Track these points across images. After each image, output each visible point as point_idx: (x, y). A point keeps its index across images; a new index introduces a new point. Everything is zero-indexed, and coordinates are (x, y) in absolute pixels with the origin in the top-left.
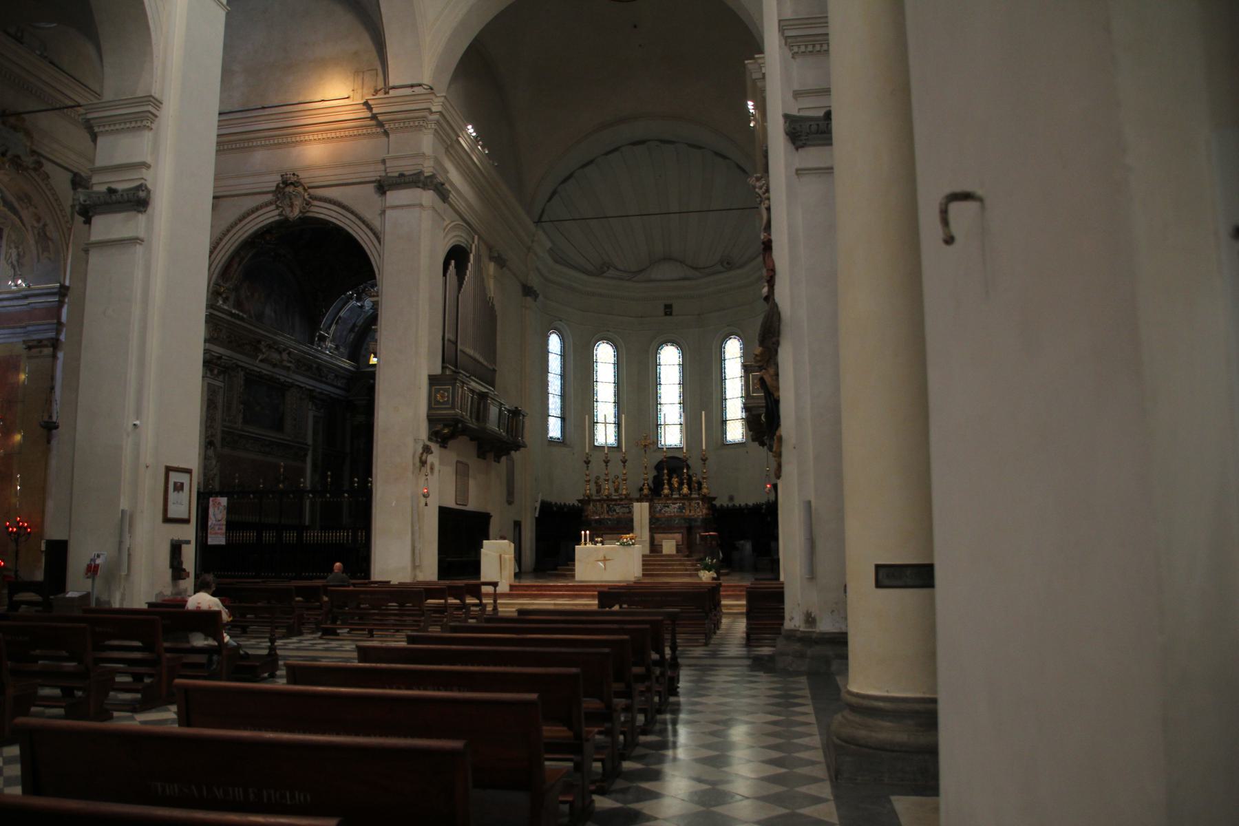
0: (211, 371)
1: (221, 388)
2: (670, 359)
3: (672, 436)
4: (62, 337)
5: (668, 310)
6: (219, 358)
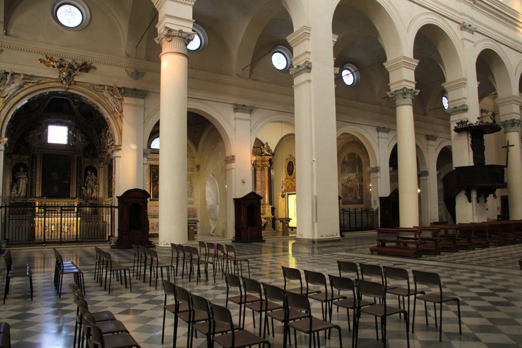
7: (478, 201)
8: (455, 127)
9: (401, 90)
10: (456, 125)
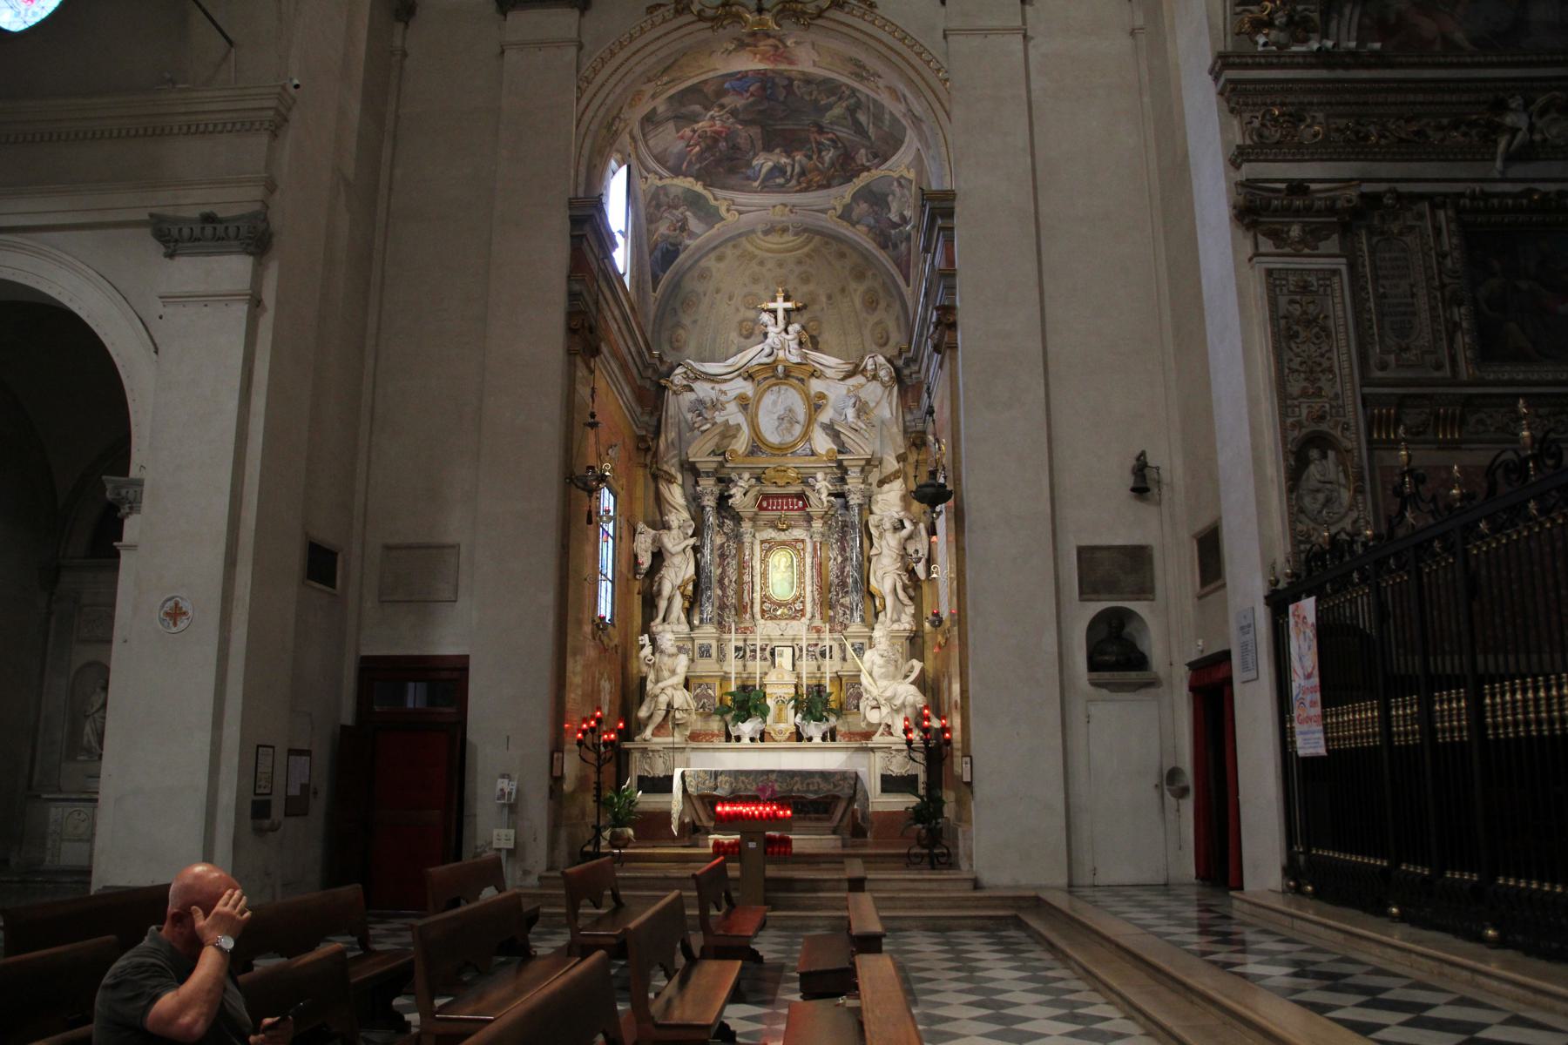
0: (1277, 236)
1: (1335, 272)
4: (958, 304)
6: (1298, 188)
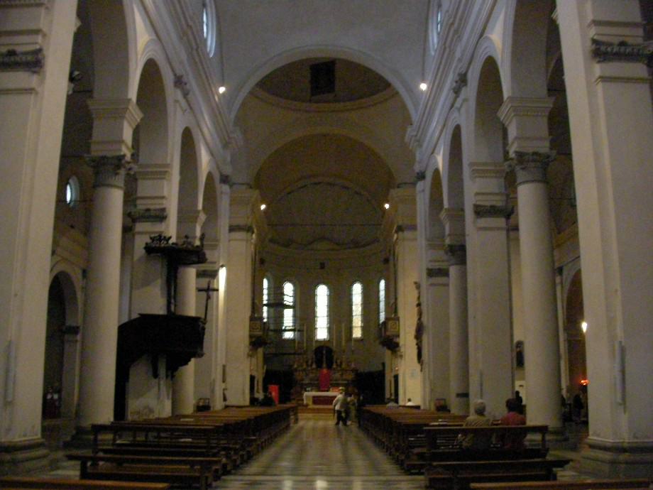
2: (322, 293)
3: (322, 333)
5: (322, 266)
7: (167, 377)
8: (147, 244)
9: (113, 158)
10: (149, 241)
